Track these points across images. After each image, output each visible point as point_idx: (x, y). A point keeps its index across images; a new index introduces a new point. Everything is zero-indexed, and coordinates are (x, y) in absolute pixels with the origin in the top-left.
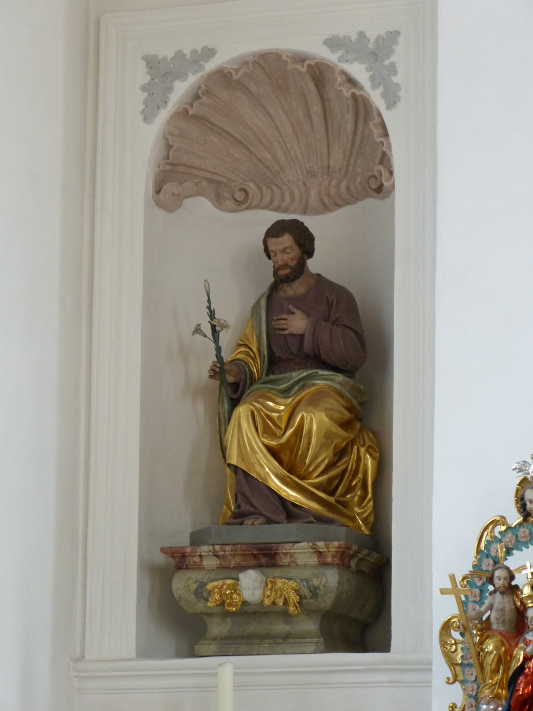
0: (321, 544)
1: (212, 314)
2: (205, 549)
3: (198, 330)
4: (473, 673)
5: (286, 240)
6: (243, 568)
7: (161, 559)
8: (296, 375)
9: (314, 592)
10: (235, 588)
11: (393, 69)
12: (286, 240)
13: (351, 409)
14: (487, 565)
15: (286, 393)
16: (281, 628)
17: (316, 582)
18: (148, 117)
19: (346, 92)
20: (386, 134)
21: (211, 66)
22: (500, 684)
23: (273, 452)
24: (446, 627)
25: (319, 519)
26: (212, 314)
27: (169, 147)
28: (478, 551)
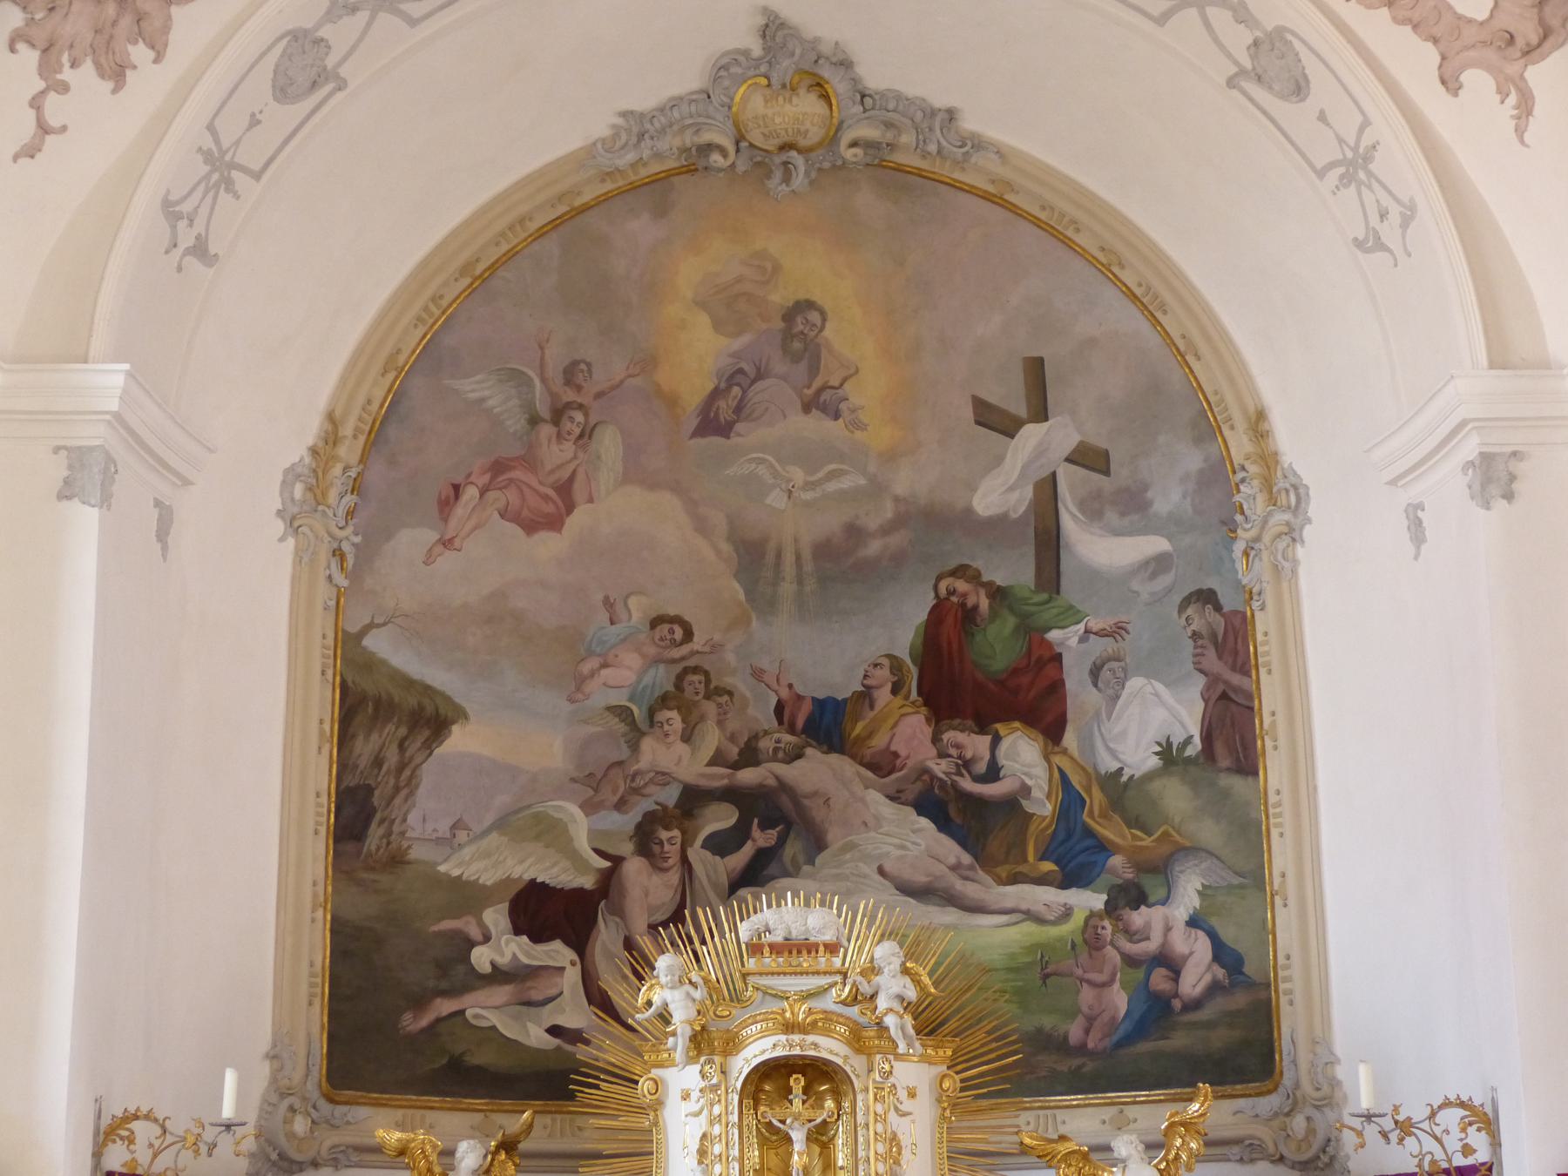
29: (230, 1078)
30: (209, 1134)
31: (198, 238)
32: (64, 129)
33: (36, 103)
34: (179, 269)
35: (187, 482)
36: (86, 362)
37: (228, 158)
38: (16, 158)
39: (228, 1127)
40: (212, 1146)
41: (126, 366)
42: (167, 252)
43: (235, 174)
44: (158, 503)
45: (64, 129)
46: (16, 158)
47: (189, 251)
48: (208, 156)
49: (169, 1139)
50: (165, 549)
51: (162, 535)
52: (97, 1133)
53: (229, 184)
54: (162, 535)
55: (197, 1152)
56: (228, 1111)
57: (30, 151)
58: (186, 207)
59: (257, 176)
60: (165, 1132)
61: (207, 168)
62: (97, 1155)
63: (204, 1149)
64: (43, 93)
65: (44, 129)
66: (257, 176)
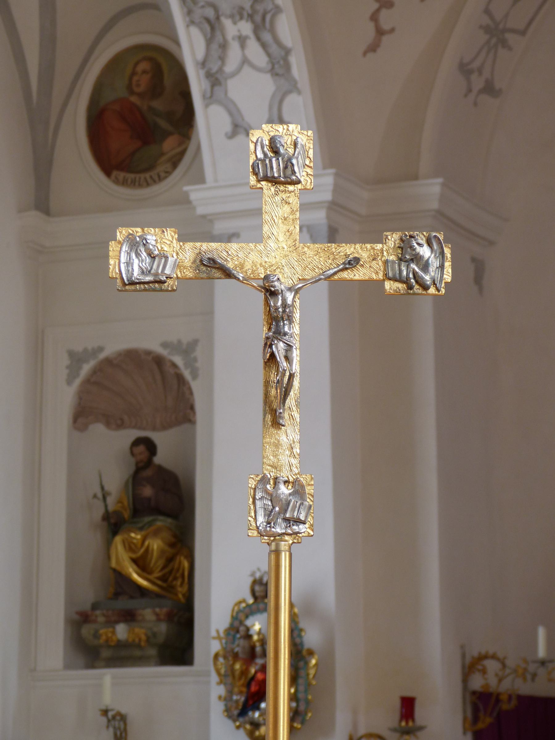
0: (157, 610)
1: (102, 488)
2: (98, 612)
3: (95, 496)
4: (229, 680)
5: (141, 448)
6: (117, 622)
7: (77, 617)
8: (147, 519)
9: (155, 635)
10: (114, 633)
11: (195, 360)
12: (141, 448)
13: (175, 536)
14: (236, 624)
15: (141, 529)
16: (138, 653)
17: (155, 629)
18: (69, 382)
19: (172, 371)
20: (191, 393)
21: (102, 356)
22: (243, 685)
23: (135, 561)
24: (216, 656)
25: (158, 596)
26: (102, 488)
27: (80, 398)
28: (232, 617)
29: (541, 633)
30: (532, 668)
31: (487, 81)
32: (392, 30)
33: (374, 17)
34: (475, 104)
35: (491, 243)
36: (416, 178)
37: (501, 26)
38: (365, 54)
39: (543, 663)
40: (534, 676)
41: (440, 180)
42: (466, 96)
43: (508, 36)
44: (474, 260)
45: (392, 30)
46: (365, 54)
47: (481, 92)
48: (487, 29)
49: (508, 671)
50: (481, 289)
51: (478, 279)
52: (463, 667)
53: (504, 43)
54: (478, 279)
55: (525, 679)
56: (542, 652)
57: (373, 48)
58: (476, 64)
59: (523, 33)
60: (504, 666)
61: (487, 37)
62: (465, 680)
63: (529, 677)
64: (378, 11)
65: (380, 32)
66: (523, 33)
